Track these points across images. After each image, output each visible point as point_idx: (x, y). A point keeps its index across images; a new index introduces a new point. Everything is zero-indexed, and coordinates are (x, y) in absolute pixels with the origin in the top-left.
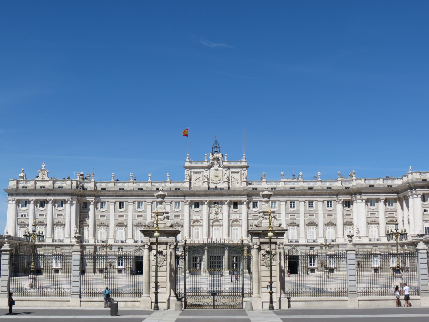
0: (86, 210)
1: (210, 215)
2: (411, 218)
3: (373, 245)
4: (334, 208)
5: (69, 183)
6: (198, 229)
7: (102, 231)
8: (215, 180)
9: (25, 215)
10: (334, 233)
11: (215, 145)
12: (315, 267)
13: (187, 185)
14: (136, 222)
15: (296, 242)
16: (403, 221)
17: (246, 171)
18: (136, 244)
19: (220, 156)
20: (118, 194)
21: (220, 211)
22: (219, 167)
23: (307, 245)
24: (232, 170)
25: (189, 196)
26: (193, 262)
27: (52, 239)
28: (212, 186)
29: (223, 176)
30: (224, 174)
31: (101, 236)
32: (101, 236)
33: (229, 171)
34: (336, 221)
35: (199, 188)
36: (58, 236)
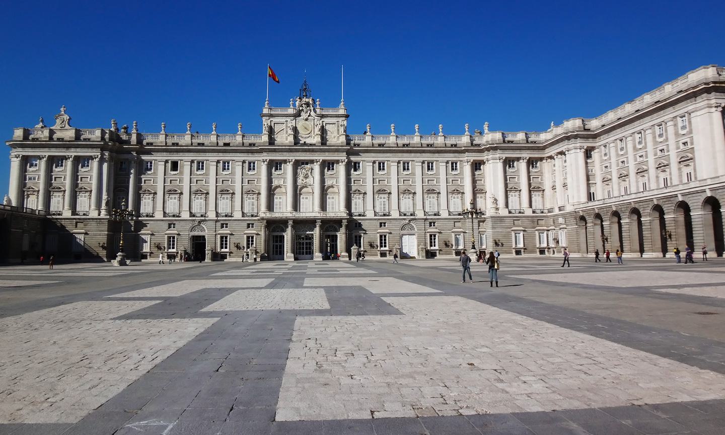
0: (124, 172)
2: (569, 181)
5: (98, 133)
6: (280, 198)
7: (147, 201)
12: (437, 247)
13: (265, 138)
15: (411, 215)
16: (554, 188)
17: (345, 122)
21: (310, 175)
22: (309, 116)
23: (426, 219)
24: (326, 120)
25: (268, 154)
26: (273, 242)
27: (72, 212)
29: (314, 127)
30: (316, 124)
32: (145, 208)
33: (323, 121)
34: (464, 189)
35: (282, 143)
36: (81, 207)
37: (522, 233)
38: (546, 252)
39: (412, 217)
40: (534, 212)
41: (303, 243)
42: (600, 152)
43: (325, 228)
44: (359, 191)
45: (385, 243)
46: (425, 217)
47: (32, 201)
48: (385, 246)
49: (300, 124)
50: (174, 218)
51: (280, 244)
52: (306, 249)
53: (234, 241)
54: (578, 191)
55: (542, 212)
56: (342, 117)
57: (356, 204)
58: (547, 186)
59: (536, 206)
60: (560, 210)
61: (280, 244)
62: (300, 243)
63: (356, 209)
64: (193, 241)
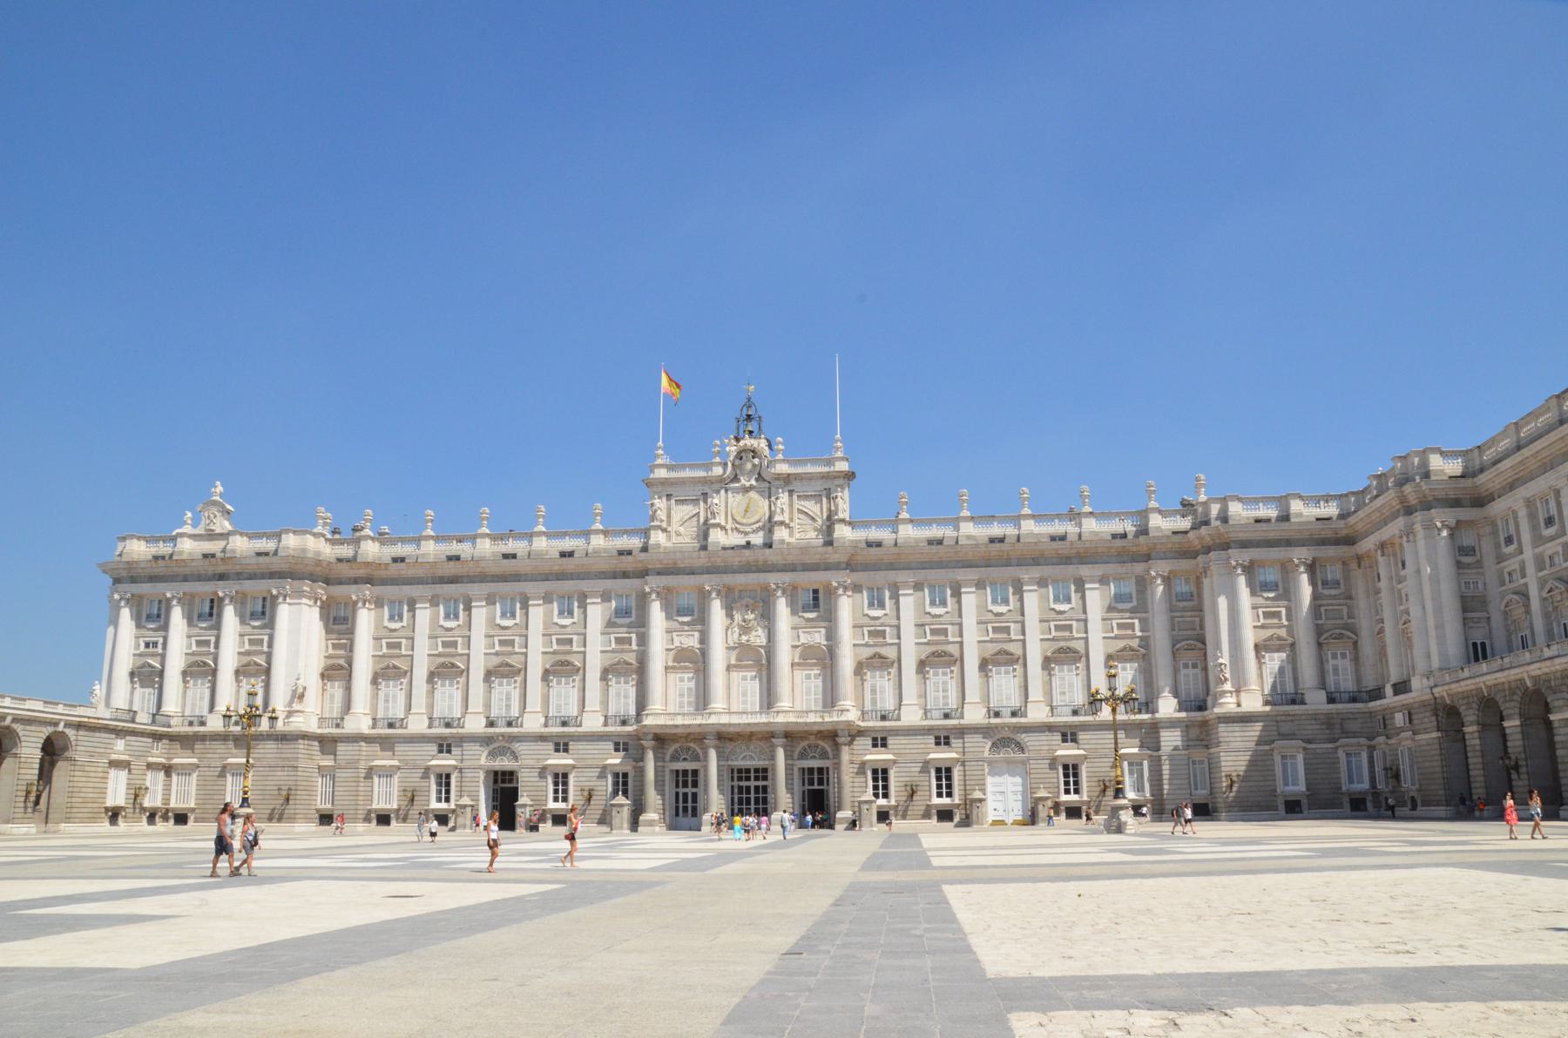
1: (729, 632)
3: (1279, 718)
4: (1138, 600)
8: (745, 521)
9: (155, 644)
10: (1143, 686)
11: (745, 413)
14: (495, 661)
15: (1014, 714)
18: (491, 730)
19: (761, 444)
20: (439, 573)
24: (796, 485)
26: (677, 786)
28: (739, 540)
31: (387, 709)
32: (387, 709)
37: (1300, 758)
38: (1369, 805)
39: (1014, 720)
40: (1331, 700)
41: (748, 788)
42: (1495, 533)
43: (797, 752)
44: (881, 657)
45: (949, 786)
46: (1052, 720)
47: (149, 694)
48: (949, 795)
49: (736, 501)
50: (448, 731)
51: (694, 790)
52: (749, 798)
53: (581, 784)
54: (1441, 639)
55: (1354, 700)
56: (839, 477)
57: (874, 691)
58: (1364, 624)
59: (1337, 684)
60: (1396, 693)
61: (694, 790)
62: (740, 788)
63: (874, 702)
64: (496, 781)
